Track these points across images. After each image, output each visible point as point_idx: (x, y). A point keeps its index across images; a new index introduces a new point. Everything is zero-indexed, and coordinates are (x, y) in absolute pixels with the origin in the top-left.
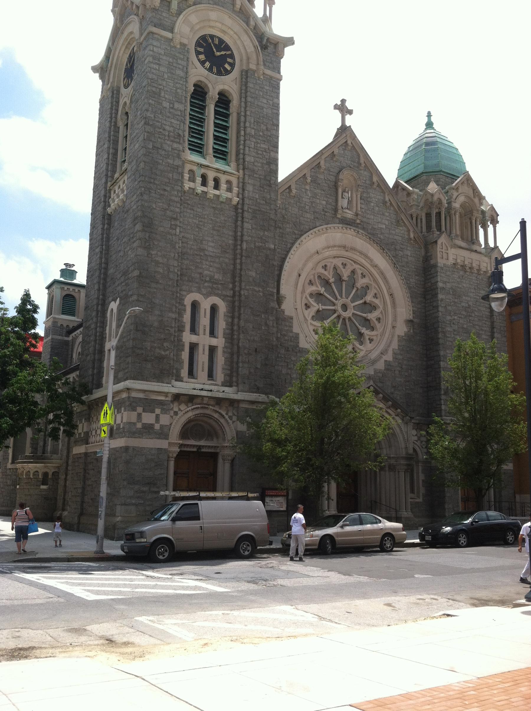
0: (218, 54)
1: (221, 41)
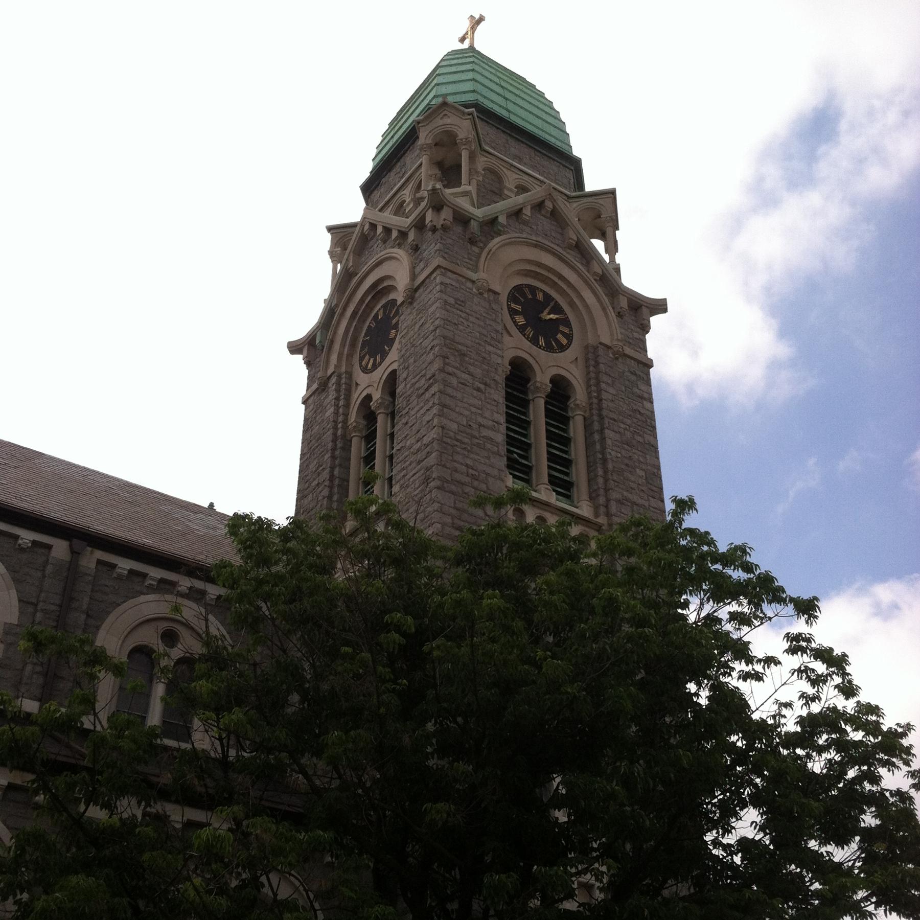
1: (548, 298)
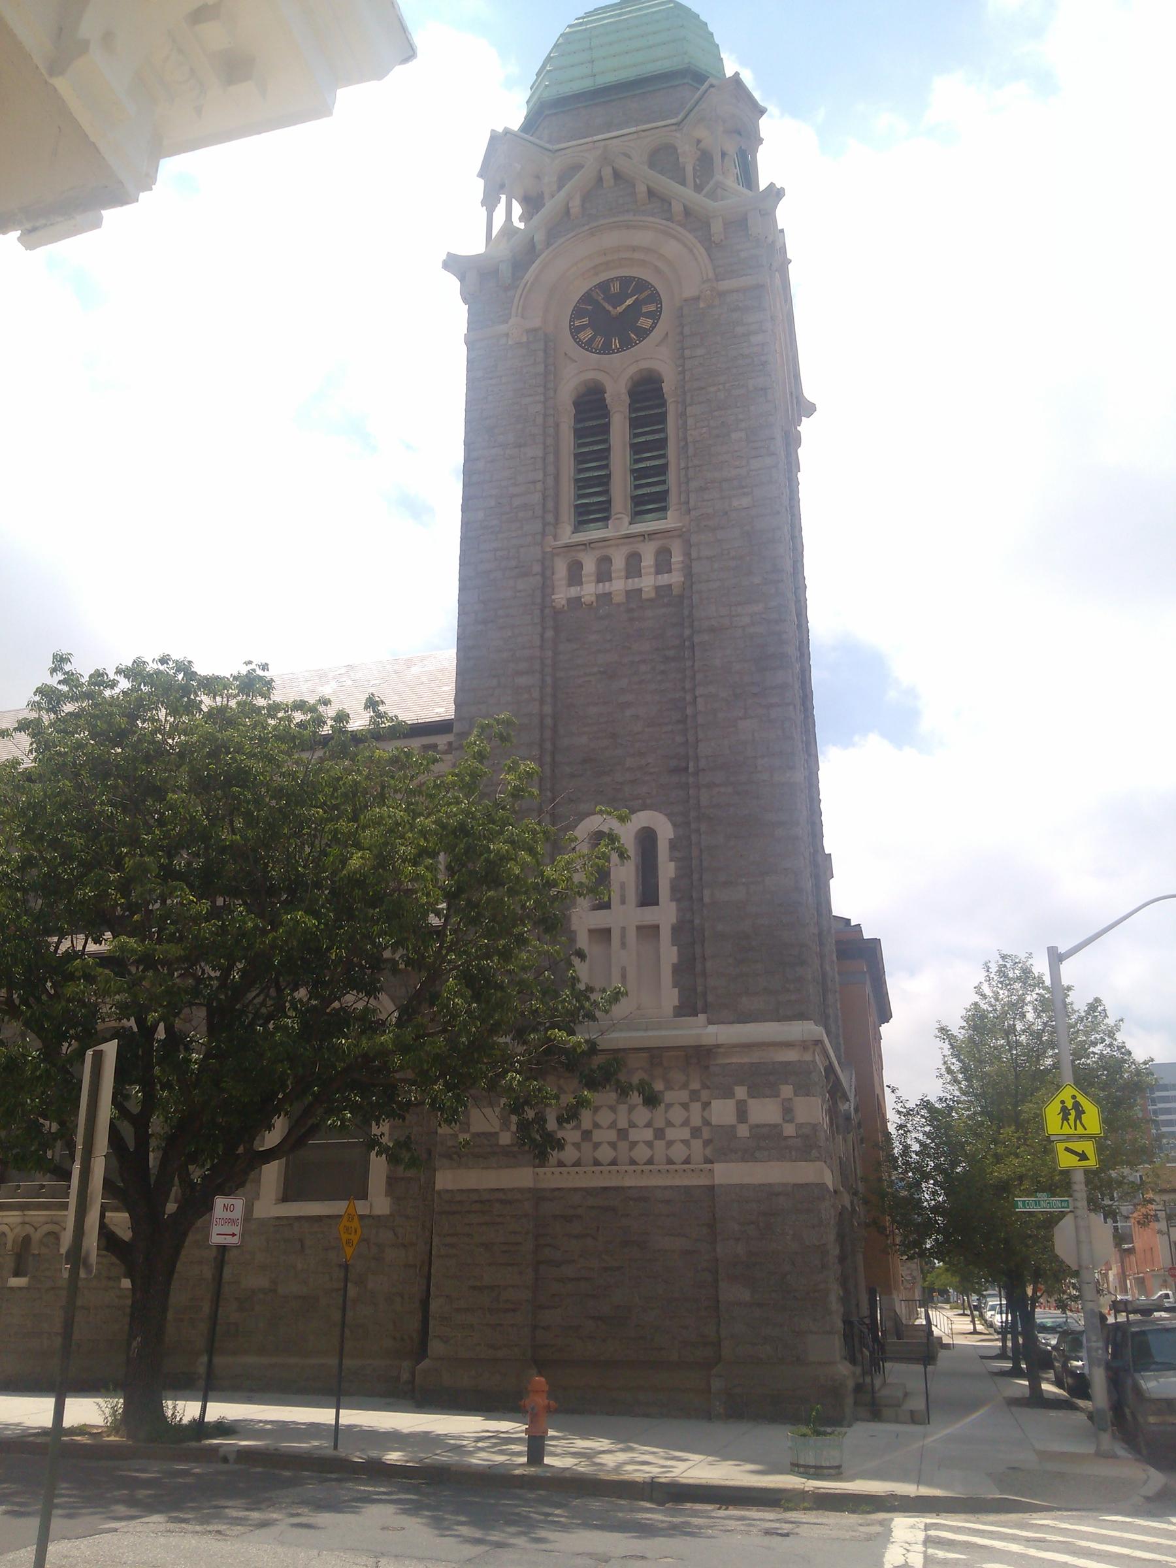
0: (620, 309)
1: (625, 281)
